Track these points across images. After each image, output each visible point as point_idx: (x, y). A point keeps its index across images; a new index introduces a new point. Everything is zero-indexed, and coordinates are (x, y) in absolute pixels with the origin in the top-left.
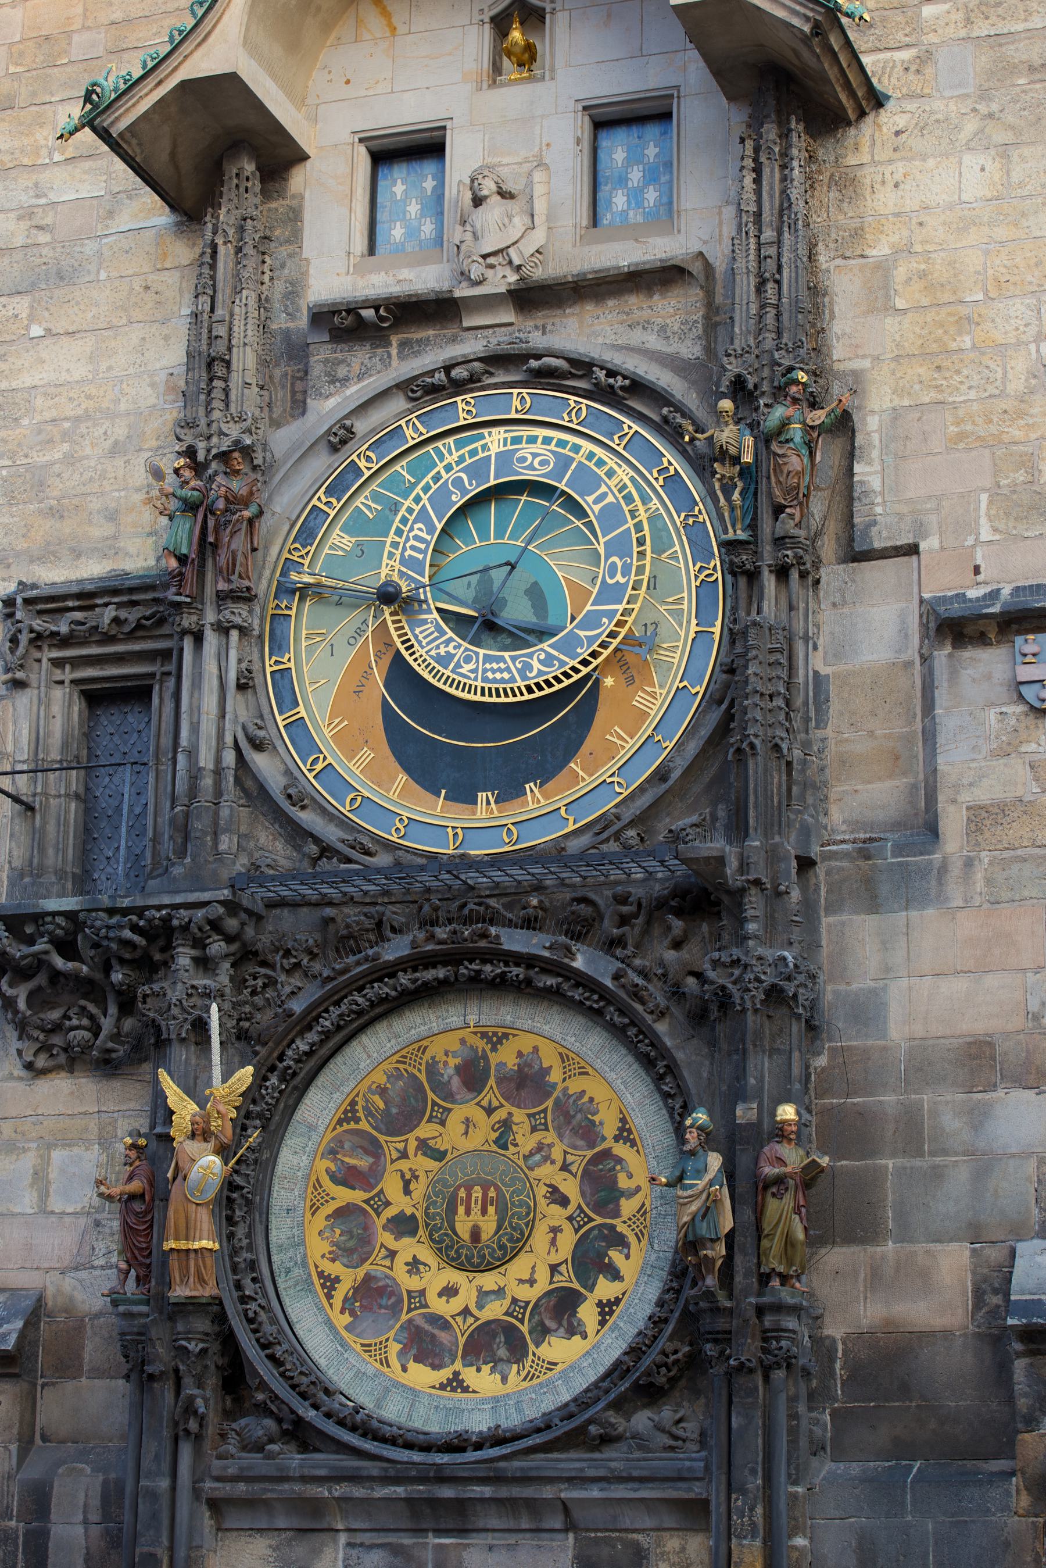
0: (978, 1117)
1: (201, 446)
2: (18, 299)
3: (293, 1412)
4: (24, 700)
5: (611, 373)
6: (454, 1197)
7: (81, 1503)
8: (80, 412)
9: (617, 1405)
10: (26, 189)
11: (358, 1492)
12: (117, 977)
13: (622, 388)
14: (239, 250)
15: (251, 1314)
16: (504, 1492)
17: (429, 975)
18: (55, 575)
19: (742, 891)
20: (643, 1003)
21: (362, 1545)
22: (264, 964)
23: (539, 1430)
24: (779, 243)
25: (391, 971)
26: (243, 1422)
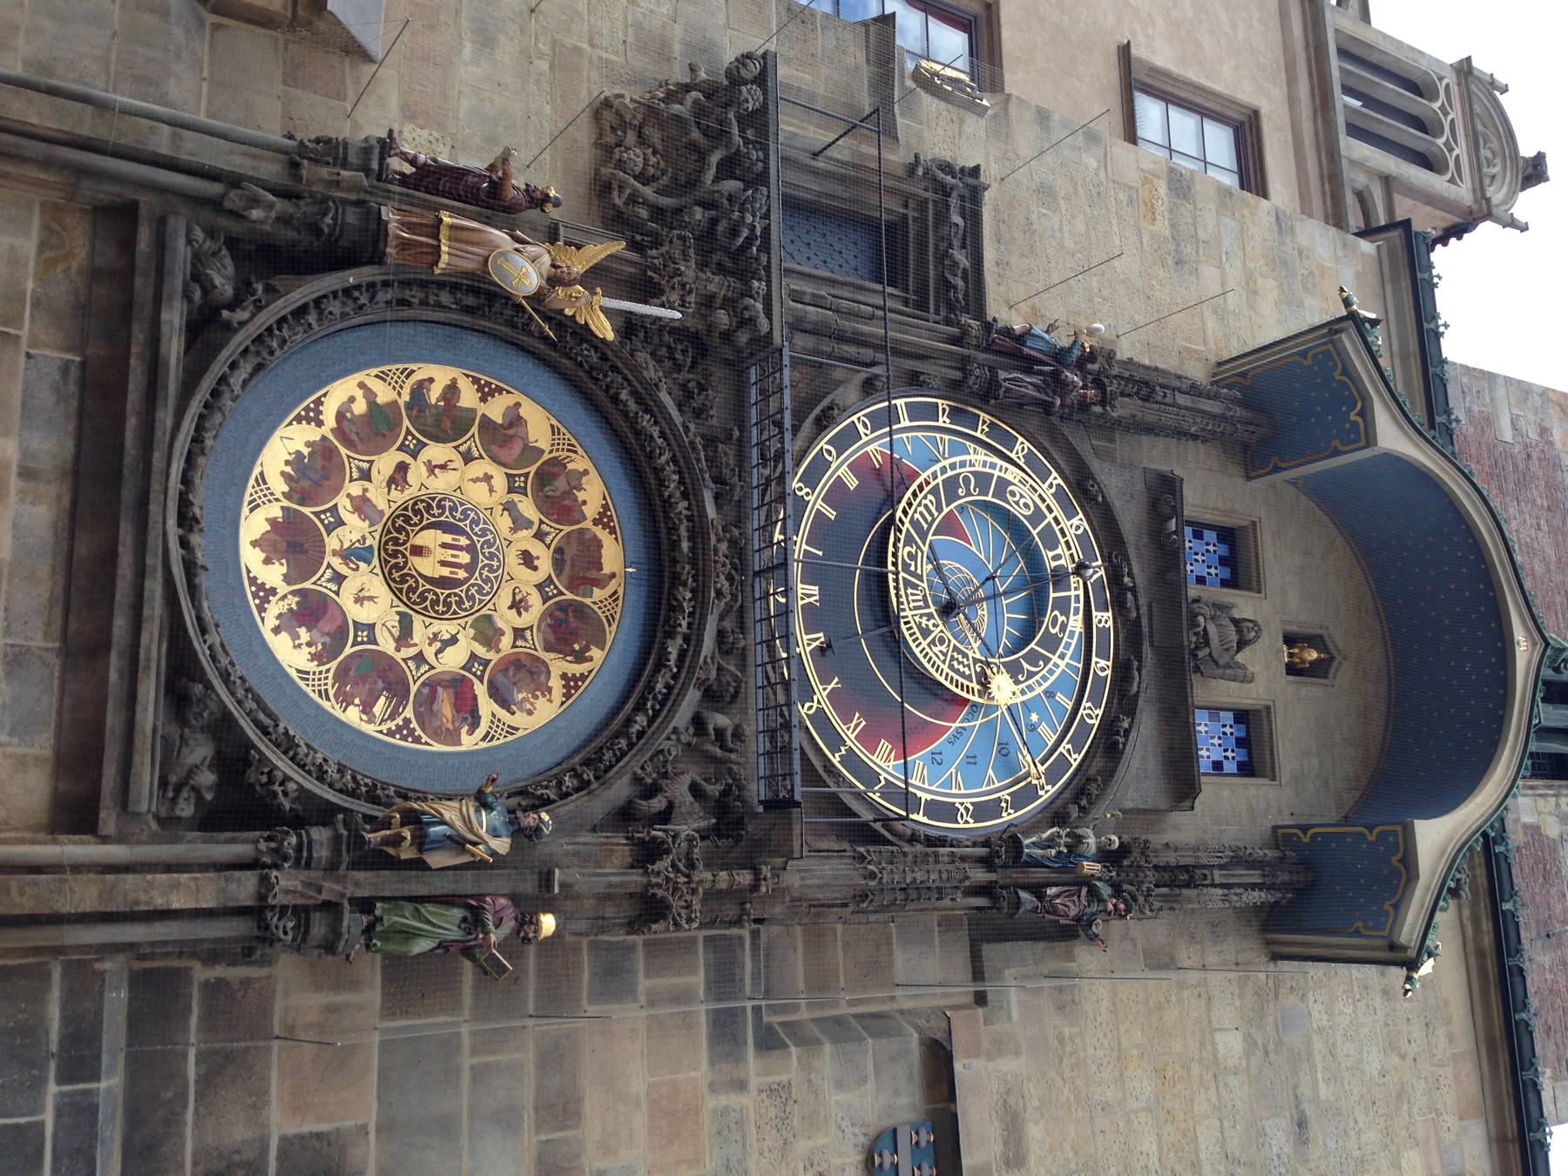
0: (507, 1120)
1: (1094, 367)
3: (242, 324)
5: (1127, 732)
12: (699, 214)
13: (1117, 743)
14: (1214, 417)
15: (356, 294)
17: (683, 532)
19: (756, 872)
20: (651, 759)
22: (694, 363)
23: (199, 619)
24: (1214, 885)
25: (690, 493)
26: (228, 261)
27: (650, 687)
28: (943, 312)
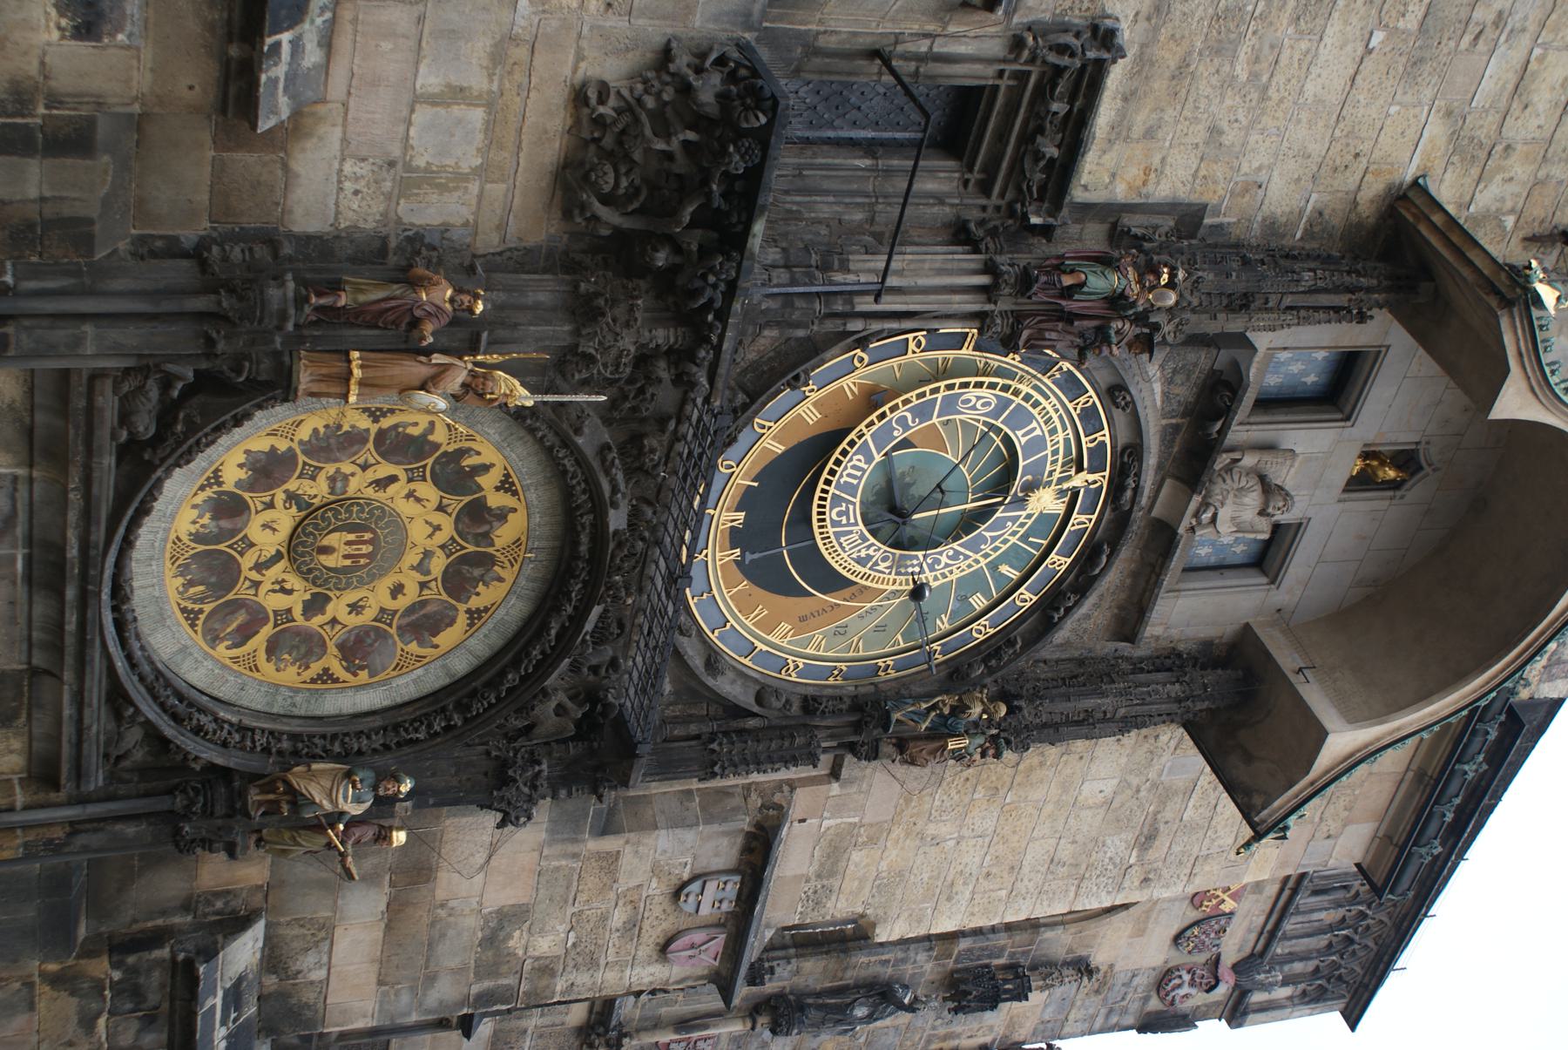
2: (1420, 15)
3: (163, 460)
4: (996, 48)
5: (1068, 610)
6: (365, 529)
7: (65, 194)
8: (1271, 92)
9: (148, 724)
10: (1526, 18)
11: (72, 516)
16: (70, 641)
17: (584, 538)
18: (1116, 77)
21: (15, 489)
24: (1111, 720)
25: (599, 510)
26: (154, 394)
27: (525, 651)
28: (1009, 196)
